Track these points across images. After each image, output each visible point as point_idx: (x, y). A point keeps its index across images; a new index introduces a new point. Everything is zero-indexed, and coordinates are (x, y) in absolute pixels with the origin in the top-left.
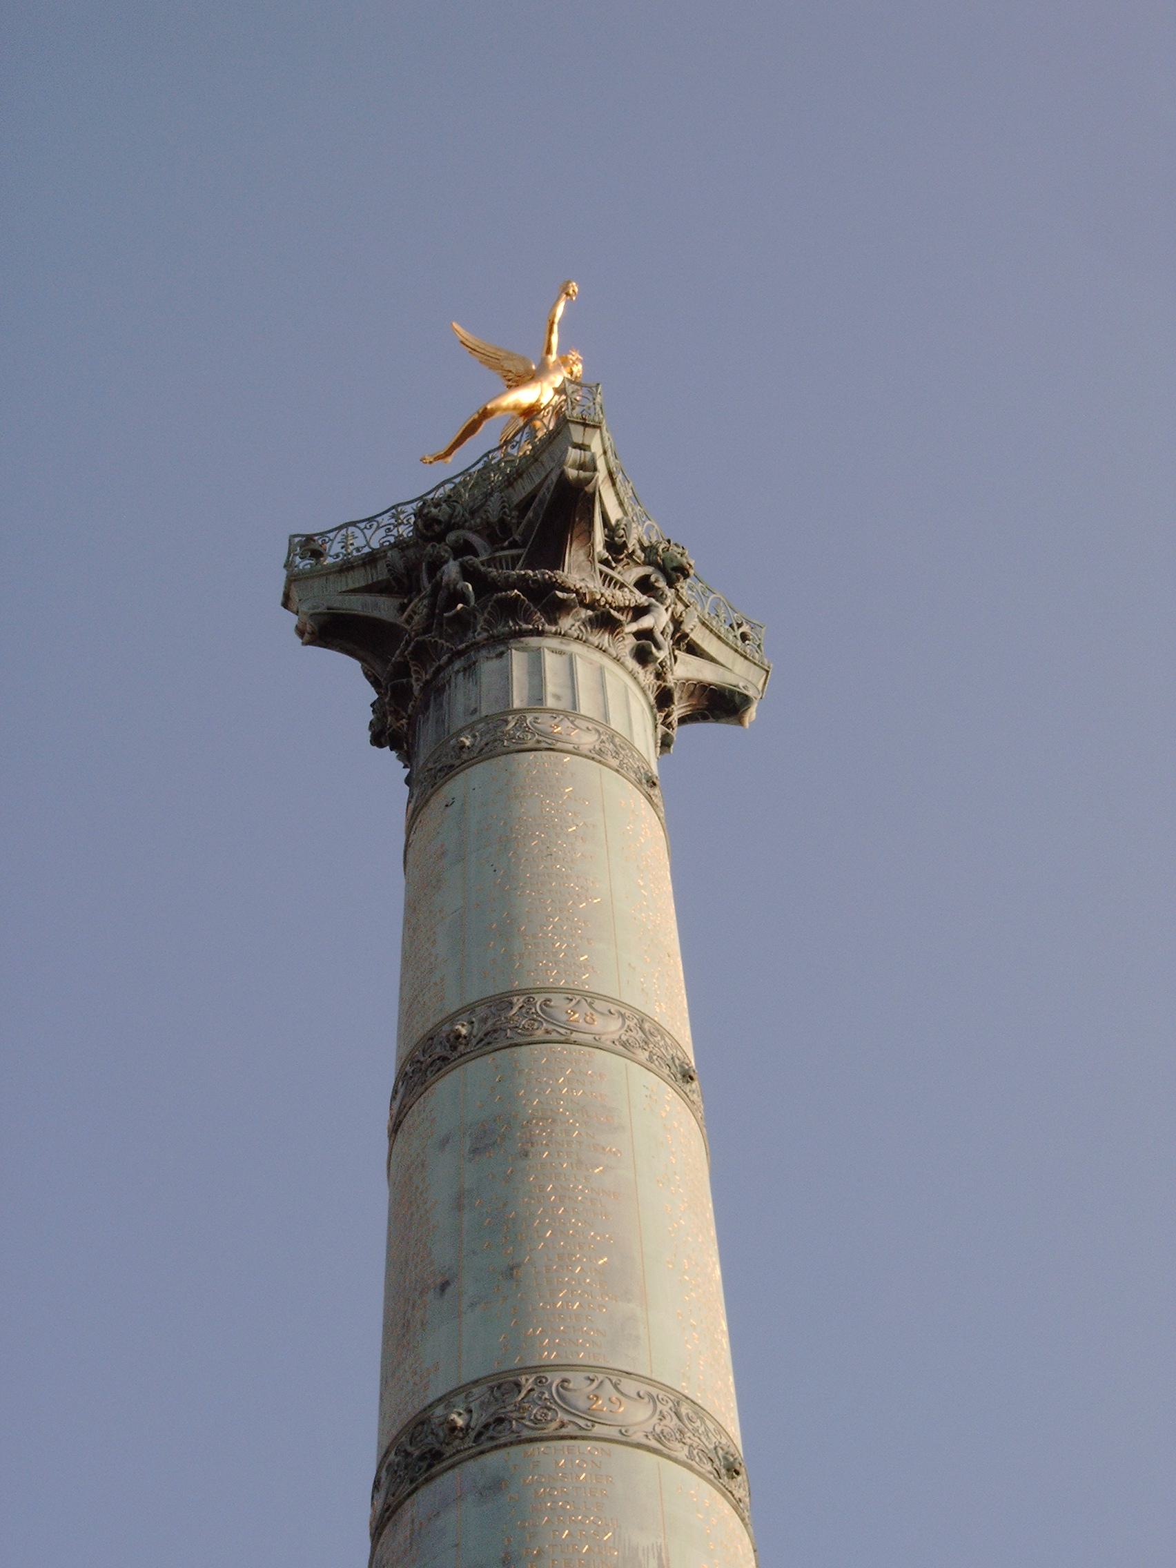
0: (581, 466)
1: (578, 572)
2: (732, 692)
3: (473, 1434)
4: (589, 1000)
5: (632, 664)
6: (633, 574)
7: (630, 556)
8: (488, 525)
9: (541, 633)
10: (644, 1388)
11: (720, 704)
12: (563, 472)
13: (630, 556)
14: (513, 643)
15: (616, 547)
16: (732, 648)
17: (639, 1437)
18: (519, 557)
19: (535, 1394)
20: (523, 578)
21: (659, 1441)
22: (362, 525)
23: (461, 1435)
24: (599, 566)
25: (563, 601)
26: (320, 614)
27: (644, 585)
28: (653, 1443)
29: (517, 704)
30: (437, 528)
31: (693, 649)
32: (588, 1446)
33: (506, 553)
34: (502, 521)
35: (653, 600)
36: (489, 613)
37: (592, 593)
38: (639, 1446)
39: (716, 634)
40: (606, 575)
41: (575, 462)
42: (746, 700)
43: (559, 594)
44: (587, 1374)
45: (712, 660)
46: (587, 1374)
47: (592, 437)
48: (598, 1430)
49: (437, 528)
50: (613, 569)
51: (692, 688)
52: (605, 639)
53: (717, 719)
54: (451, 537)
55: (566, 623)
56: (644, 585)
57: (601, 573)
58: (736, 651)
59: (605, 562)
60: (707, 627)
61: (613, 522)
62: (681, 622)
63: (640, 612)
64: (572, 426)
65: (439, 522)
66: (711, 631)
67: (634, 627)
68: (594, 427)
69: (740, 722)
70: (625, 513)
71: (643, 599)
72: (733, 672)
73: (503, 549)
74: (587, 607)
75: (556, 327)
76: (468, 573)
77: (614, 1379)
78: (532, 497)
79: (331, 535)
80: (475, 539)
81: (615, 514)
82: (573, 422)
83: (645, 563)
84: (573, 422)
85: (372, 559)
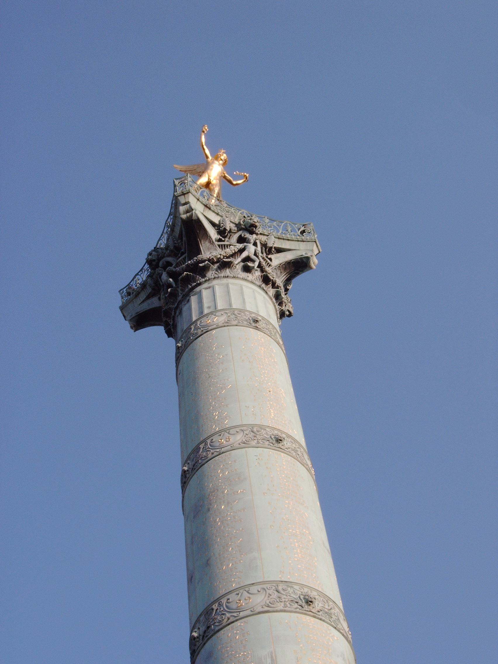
0: (187, 212)
1: (208, 252)
2: (301, 259)
3: (201, 637)
4: (227, 431)
5: (245, 275)
6: (235, 237)
7: (230, 231)
8: (172, 251)
9: (200, 284)
10: (259, 587)
11: (298, 267)
12: (181, 219)
13: (230, 231)
14: (192, 294)
15: (222, 232)
16: (296, 241)
17: (260, 609)
18: (185, 257)
19: (218, 611)
20: (188, 266)
21: (268, 606)
22: (140, 274)
23: (198, 640)
24: (217, 243)
25: (204, 266)
26: (133, 318)
27: (241, 240)
28: (266, 609)
29: (194, 319)
30: (154, 263)
31: (279, 250)
32: (238, 623)
33: (181, 258)
34: (175, 247)
35: (245, 244)
36: (181, 286)
37: (215, 257)
38: (259, 613)
39: (286, 239)
40: (222, 245)
41: (184, 211)
42: (308, 258)
43: (201, 265)
44: (236, 593)
45: (289, 250)
46: (236, 593)
47: (188, 197)
48: (242, 614)
49: (154, 263)
50: (224, 241)
51: (284, 266)
53: (303, 271)
54: (161, 264)
55: (210, 274)
56: (241, 240)
57: (219, 246)
58: (298, 241)
59: (220, 240)
60: (281, 239)
61: (217, 222)
62: (266, 244)
63: (242, 251)
64: (179, 198)
65: (154, 260)
66: (284, 239)
67: (239, 259)
68: (188, 193)
69: (311, 268)
70: (222, 216)
71: (241, 246)
72: (299, 250)
73: (180, 257)
74: (217, 262)
75: (205, 147)
76: (171, 275)
77: (247, 589)
78: (181, 232)
79: (132, 283)
80: (170, 259)
81: (216, 220)
82: (179, 196)
83: (238, 231)
84: (179, 196)
85: (144, 286)
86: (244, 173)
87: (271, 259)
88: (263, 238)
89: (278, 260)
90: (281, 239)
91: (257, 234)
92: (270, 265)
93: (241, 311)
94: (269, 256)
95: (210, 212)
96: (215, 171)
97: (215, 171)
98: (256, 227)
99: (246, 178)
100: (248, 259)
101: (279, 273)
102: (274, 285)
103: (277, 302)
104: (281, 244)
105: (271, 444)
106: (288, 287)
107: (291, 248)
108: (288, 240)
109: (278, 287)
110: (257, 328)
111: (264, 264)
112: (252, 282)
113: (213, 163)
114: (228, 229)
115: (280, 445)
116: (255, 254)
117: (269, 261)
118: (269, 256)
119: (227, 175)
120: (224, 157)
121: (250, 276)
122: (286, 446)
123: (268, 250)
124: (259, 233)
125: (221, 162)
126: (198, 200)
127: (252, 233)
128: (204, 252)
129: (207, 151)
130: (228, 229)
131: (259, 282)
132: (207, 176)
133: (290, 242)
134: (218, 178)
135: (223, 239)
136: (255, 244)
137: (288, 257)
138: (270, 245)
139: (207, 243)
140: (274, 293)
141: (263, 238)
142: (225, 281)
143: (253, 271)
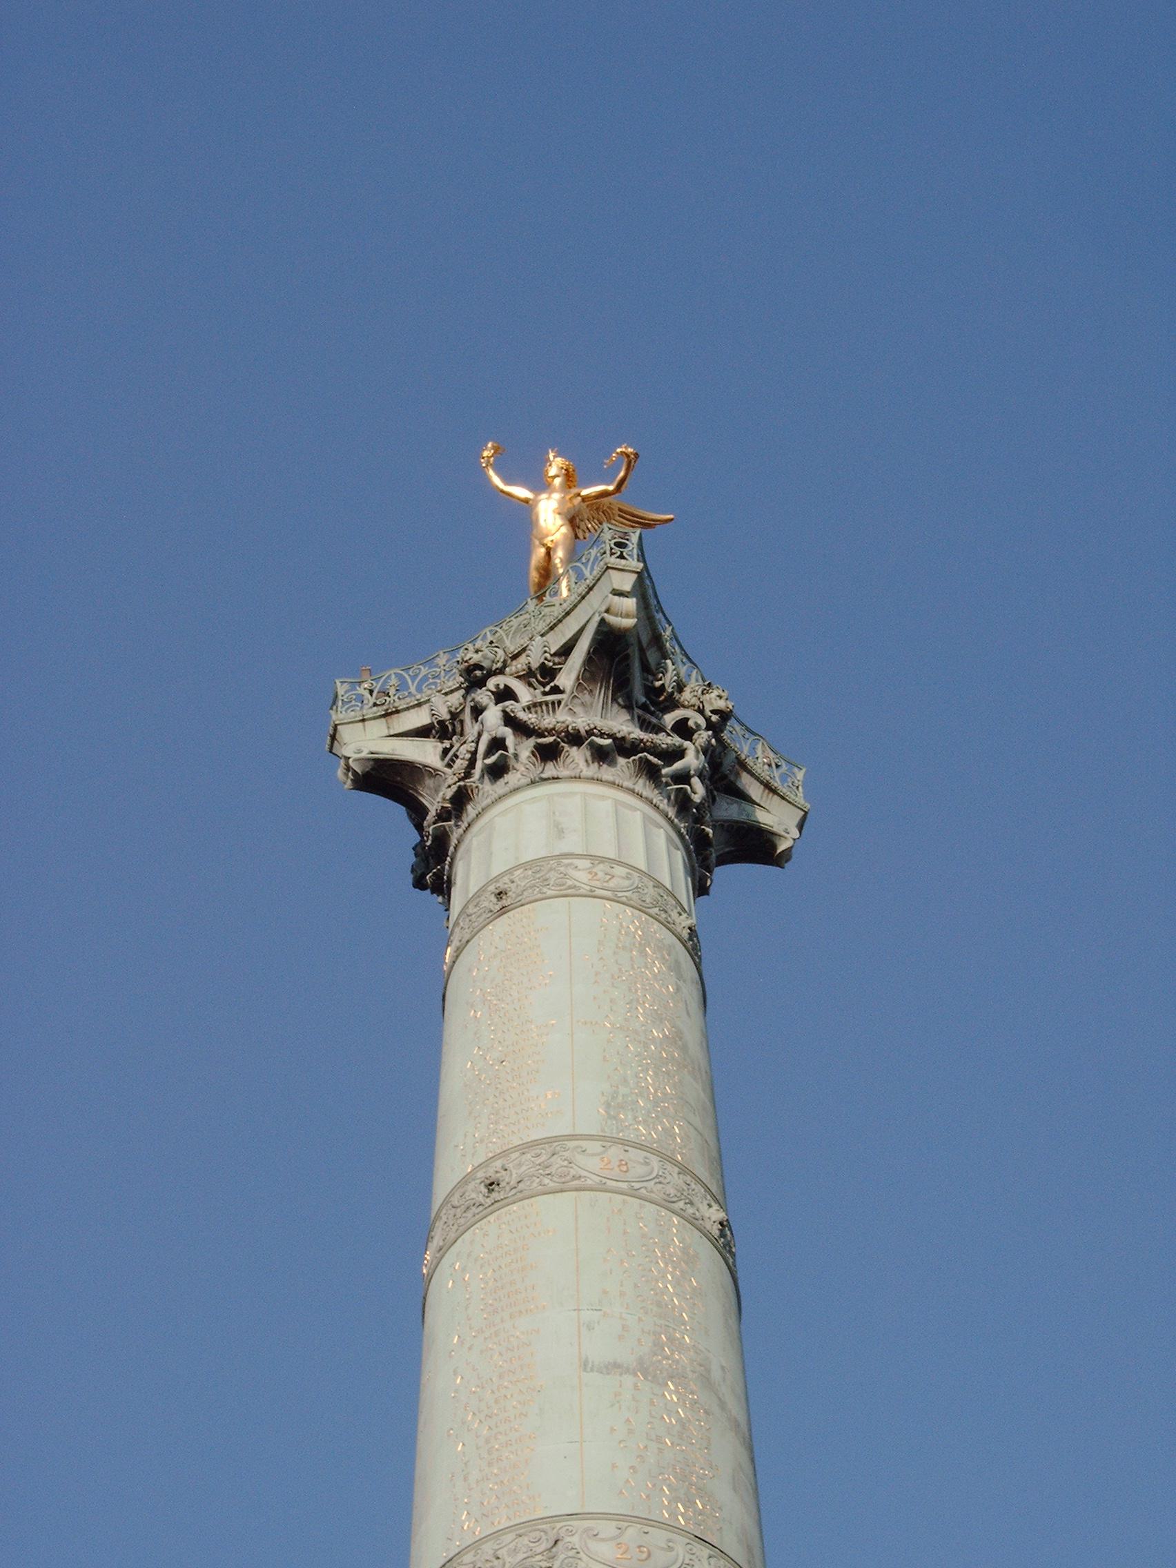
0: (348, 768)
5: (500, 787)
6: (467, 716)
13: (454, 716)
16: (580, 602)
25: (436, 838)
31: (566, 651)
39: (564, 617)
42: (603, 621)
50: (452, 746)
51: (587, 675)
52: (471, 810)
58: (583, 598)
60: (555, 625)
62: (529, 668)
66: (560, 621)
71: (477, 727)
81: (420, 718)
86: (615, 451)
87: (556, 690)
88: (519, 665)
91: (501, 671)
92: (559, 702)
93: (477, 895)
94: (547, 688)
95: (401, 715)
96: (549, 515)
97: (549, 515)
98: (478, 666)
99: (628, 456)
100: (497, 744)
101: (586, 697)
102: (576, 739)
103: (612, 763)
105: (481, 1208)
106: (658, 684)
108: (568, 614)
109: (590, 733)
110: (503, 910)
112: (516, 790)
113: (536, 502)
115: (495, 1195)
116: (509, 720)
117: (550, 698)
118: (547, 688)
119: (585, 492)
120: (555, 466)
121: (512, 778)
122: (513, 1183)
123: (547, 673)
124: (499, 665)
125: (557, 481)
127: (481, 683)
129: (521, 492)
131: (536, 770)
132: (537, 542)
134: (559, 521)
138: (535, 665)
140: (588, 754)
141: (519, 665)
142: (469, 836)
143: (512, 762)
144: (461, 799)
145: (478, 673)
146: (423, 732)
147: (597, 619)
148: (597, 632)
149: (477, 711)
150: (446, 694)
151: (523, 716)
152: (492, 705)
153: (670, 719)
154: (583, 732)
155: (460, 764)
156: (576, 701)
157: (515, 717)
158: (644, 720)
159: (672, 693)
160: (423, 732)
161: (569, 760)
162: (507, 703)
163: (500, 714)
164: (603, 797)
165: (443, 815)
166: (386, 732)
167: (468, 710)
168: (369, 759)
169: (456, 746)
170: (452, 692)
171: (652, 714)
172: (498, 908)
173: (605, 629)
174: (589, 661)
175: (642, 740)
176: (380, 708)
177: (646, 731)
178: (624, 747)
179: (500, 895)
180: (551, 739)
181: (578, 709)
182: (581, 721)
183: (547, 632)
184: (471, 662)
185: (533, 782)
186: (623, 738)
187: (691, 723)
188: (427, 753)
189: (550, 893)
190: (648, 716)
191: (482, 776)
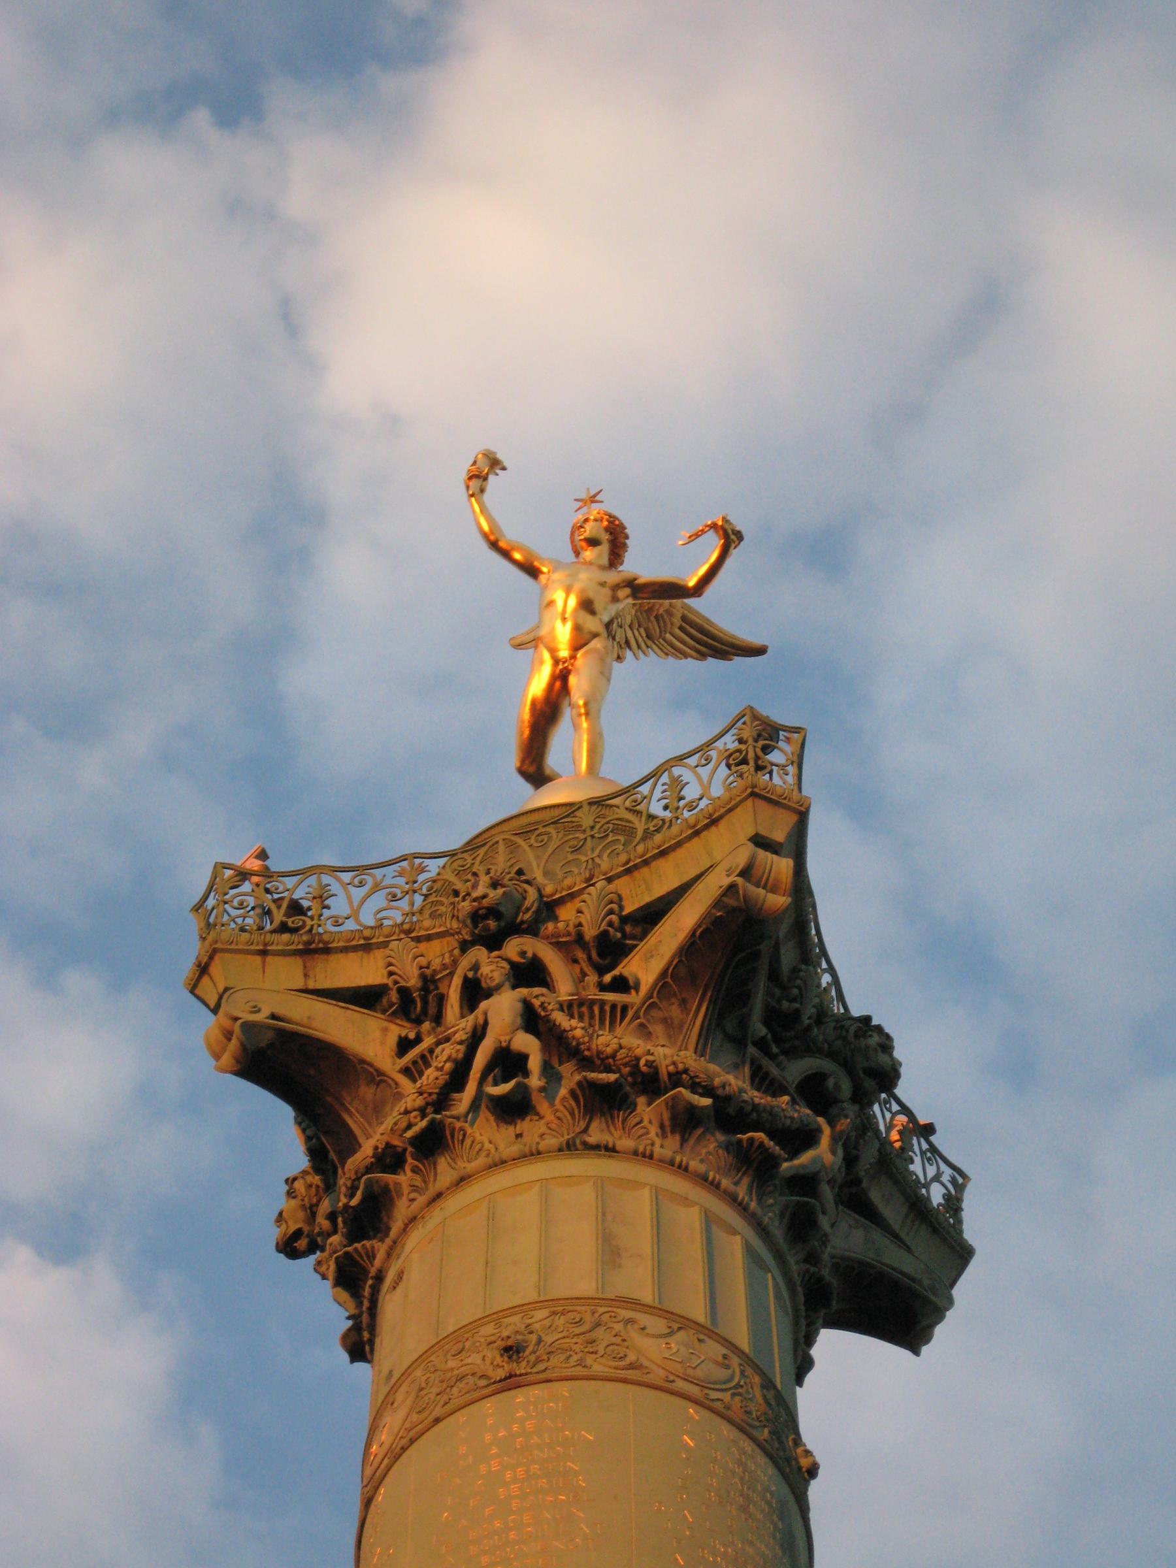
9: (380, 1278)
13: (429, 982)
16: (689, 838)
35: (484, 1005)
39: (655, 857)
45: (683, 890)
50: (418, 1040)
51: (683, 971)
52: (445, 1170)
55: (402, 1210)
57: (406, 1071)
58: (697, 833)
60: (636, 867)
65: (298, 1234)
66: (646, 863)
81: (365, 972)
87: (622, 985)
89: (645, 966)
90: (636, 867)
92: (625, 1008)
94: (608, 978)
95: (337, 960)
101: (675, 1011)
102: (650, 1082)
104: (648, 889)
107: (686, 878)
108: (663, 853)
109: (676, 1079)
110: (510, 1382)
111: (578, 1033)
114: (413, 982)
117: (610, 997)
118: (608, 978)
126: (264, 953)
128: (364, 1130)
130: (413, 981)
133: (672, 856)
135: (412, 1036)
136: (529, 973)
137: (684, 920)
139: (368, 1092)
140: (666, 1116)
144: (432, 1143)
145: (492, 924)
146: (365, 998)
147: (716, 882)
148: (718, 904)
149: (474, 992)
150: (418, 940)
151: (561, 1019)
152: (507, 985)
153: (796, 1070)
154: (664, 1076)
155: (432, 1077)
156: (654, 1013)
157: (547, 1019)
158: (760, 1067)
159: (809, 1028)
160: (365, 998)
161: (633, 1120)
162: (537, 990)
163: (519, 1006)
164: (686, 1201)
165: (389, 1159)
166: (300, 983)
167: (457, 981)
168: (268, 1027)
169: (428, 1042)
170: (429, 938)
171: (772, 1057)
172: (501, 1373)
173: (731, 902)
174: (691, 949)
175: (755, 1107)
176: (295, 937)
177: (766, 1092)
178: (729, 1116)
179: (512, 1351)
180: (612, 1077)
181: (658, 1029)
182: (664, 1053)
183: (619, 876)
184: (485, 902)
185: (569, 1148)
186: (728, 1098)
187: (830, 1083)
188: (370, 1038)
189: (597, 1368)
190: (765, 1062)
191: (475, 1106)
